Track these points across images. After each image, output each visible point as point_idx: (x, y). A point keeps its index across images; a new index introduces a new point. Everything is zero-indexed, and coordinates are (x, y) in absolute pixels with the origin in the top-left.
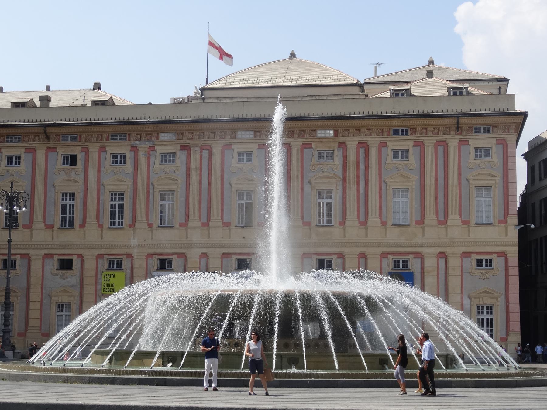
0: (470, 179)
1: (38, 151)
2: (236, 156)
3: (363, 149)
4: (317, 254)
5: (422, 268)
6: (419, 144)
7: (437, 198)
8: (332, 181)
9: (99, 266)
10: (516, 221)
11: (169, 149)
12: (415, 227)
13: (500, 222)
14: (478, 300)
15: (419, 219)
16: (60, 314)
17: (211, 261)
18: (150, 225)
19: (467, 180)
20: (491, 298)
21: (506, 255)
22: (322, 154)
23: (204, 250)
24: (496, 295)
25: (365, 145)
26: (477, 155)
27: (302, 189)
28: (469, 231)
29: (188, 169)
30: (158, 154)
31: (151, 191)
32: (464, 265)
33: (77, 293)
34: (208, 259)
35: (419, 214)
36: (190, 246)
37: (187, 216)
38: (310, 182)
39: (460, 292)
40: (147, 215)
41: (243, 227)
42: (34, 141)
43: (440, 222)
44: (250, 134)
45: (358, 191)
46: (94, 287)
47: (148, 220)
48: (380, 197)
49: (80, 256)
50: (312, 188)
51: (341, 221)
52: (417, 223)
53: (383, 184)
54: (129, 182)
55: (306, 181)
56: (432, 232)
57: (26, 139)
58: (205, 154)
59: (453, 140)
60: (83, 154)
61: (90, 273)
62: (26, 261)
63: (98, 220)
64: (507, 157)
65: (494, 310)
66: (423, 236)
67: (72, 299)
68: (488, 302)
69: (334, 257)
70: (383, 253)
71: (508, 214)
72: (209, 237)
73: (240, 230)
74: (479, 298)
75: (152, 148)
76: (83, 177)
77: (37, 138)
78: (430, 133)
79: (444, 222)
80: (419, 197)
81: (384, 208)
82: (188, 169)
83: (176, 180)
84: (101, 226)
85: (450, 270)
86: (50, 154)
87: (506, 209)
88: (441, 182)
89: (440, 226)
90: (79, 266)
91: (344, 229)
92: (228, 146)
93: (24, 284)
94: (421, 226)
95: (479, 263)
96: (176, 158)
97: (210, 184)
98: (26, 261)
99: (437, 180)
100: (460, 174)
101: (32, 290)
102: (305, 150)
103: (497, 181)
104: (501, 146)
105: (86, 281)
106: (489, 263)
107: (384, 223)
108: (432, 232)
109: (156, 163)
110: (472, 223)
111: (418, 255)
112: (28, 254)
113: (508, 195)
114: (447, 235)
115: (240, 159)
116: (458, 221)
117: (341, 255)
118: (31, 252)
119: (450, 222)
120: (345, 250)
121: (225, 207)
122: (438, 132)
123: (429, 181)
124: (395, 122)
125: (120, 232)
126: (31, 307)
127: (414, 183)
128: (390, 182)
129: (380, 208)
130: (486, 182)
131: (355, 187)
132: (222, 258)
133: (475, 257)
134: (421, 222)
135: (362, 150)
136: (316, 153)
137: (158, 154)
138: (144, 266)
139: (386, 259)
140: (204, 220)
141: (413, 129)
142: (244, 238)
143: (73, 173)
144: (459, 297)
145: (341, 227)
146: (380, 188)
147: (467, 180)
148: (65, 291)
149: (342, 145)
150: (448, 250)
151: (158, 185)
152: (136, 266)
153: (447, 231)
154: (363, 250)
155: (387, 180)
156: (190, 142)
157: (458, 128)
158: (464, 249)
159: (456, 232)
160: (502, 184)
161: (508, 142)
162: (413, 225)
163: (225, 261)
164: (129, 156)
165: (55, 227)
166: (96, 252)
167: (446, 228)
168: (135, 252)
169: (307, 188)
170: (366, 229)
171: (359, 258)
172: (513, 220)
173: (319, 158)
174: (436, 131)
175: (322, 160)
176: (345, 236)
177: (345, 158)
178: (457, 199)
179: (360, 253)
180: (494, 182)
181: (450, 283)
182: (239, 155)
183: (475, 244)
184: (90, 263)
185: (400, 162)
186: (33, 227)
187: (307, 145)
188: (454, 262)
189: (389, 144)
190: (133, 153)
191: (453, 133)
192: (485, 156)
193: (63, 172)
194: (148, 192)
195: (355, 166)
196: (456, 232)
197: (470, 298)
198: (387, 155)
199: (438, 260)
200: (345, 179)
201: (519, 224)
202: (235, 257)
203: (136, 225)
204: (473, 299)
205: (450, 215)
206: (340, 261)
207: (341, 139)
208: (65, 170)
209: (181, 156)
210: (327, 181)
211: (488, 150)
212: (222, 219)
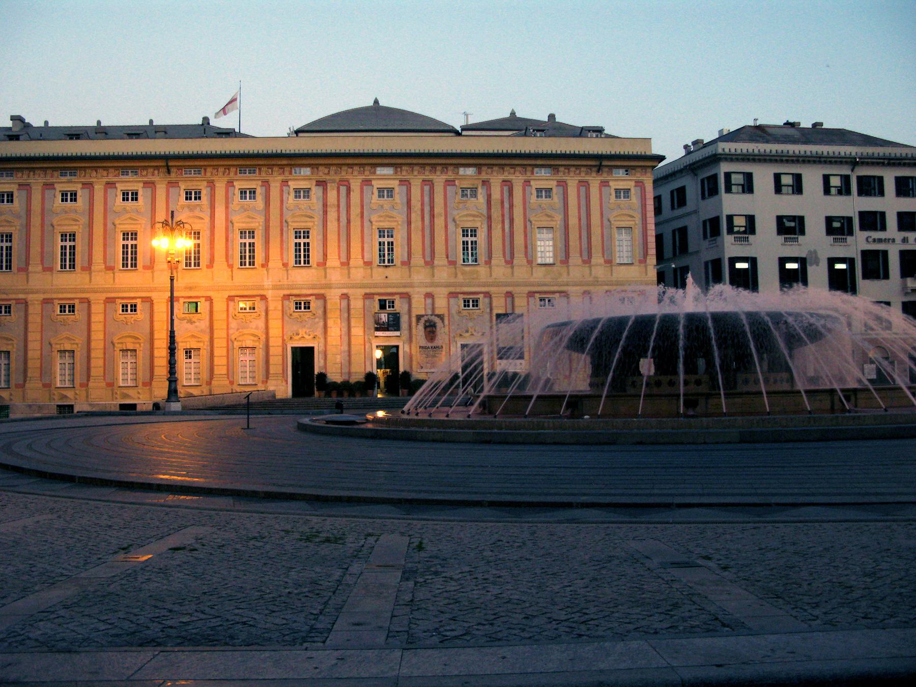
1: (158, 186)
2: (376, 192)
6: (563, 184)
7: (580, 237)
9: (231, 309)
10: (654, 261)
11: (303, 185)
13: (640, 262)
16: (189, 360)
17: (352, 303)
18: (285, 265)
23: (345, 291)
26: (616, 197)
27: (446, 227)
29: (325, 205)
30: (291, 189)
31: (285, 229)
33: (206, 338)
34: (349, 300)
35: (563, 255)
36: (329, 286)
37: (325, 255)
38: (454, 220)
40: (282, 254)
41: (386, 266)
42: (153, 175)
43: (584, 262)
44: (388, 171)
45: (503, 230)
46: (225, 331)
47: (282, 259)
48: (526, 236)
49: (209, 299)
50: (456, 226)
52: (562, 262)
53: (528, 223)
54: (261, 219)
56: (577, 271)
57: (145, 173)
58: (343, 189)
59: (595, 181)
60: (209, 189)
61: (220, 315)
62: (148, 304)
63: (227, 260)
66: (568, 274)
67: (202, 344)
69: (481, 296)
70: (529, 292)
72: (349, 277)
73: (381, 270)
75: (285, 183)
76: (209, 214)
77: (156, 172)
79: (587, 261)
81: (529, 247)
82: (325, 205)
83: (311, 217)
84: (231, 266)
86: (171, 189)
88: (584, 221)
90: (208, 308)
91: (490, 268)
92: (367, 182)
93: (148, 331)
96: (312, 193)
97: (349, 222)
98: (148, 305)
99: (580, 219)
101: (156, 336)
102: (448, 188)
104: (639, 188)
105: (216, 325)
107: (530, 262)
109: (291, 199)
112: (150, 298)
113: (646, 236)
115: (381, 195)
116: (602, 261)
117: (488, 295)
118: (154, 295)
119: (593, 261)
120: (492, 290)
121: (366, 246)
123: (573, 221)
125: (250, 271)
126: (156, 353)
129: (526, 247)
131: (500, 226)
134: (566, 261)
135: (506, 189)
137: (291, 189)
138: (280, 307)
140: (344, 260)
143: (198, 209)
146: (525, 227)
148: (193, 336)
149: (485, 183)
150: (591, 288)
152: (271, 308)
153: (591, 270)
154: (509, 289)
156: (328, 177)
157: (599, 169)
159: (600, 272)
160: (641, 226)
162: (558, 264)
163: (367, 302)
164: (259, 191)
165: (180, 268)
166: (226, 294)
167: (590, 267)
168: (269, 294)
169: (451, 226)
170: (512, 268)
172: (652, 260)
173: (463, 196)
175: (464, 199)
176: (491, 276)
177: (489, 197)
178: (600, 238)
179: (507, 293)
182: (379, 192)
184: (220, 306)
185: (544, 200)
186: (155, 268)
187: (450, 183)
189: (532, 183)
190: (264, 188)
191: (594, 174)
193: (186, 209)
194: (282, 230)
195: (499, 206)
200: (489, 218)
201: (658, 263)
202: (377, 298)
203: (270, 264)
206: (487, 300)
207: (484, 176)
208: (188, 207)
209: (316, 192)
210: (471, 219)
212: (363, 257)
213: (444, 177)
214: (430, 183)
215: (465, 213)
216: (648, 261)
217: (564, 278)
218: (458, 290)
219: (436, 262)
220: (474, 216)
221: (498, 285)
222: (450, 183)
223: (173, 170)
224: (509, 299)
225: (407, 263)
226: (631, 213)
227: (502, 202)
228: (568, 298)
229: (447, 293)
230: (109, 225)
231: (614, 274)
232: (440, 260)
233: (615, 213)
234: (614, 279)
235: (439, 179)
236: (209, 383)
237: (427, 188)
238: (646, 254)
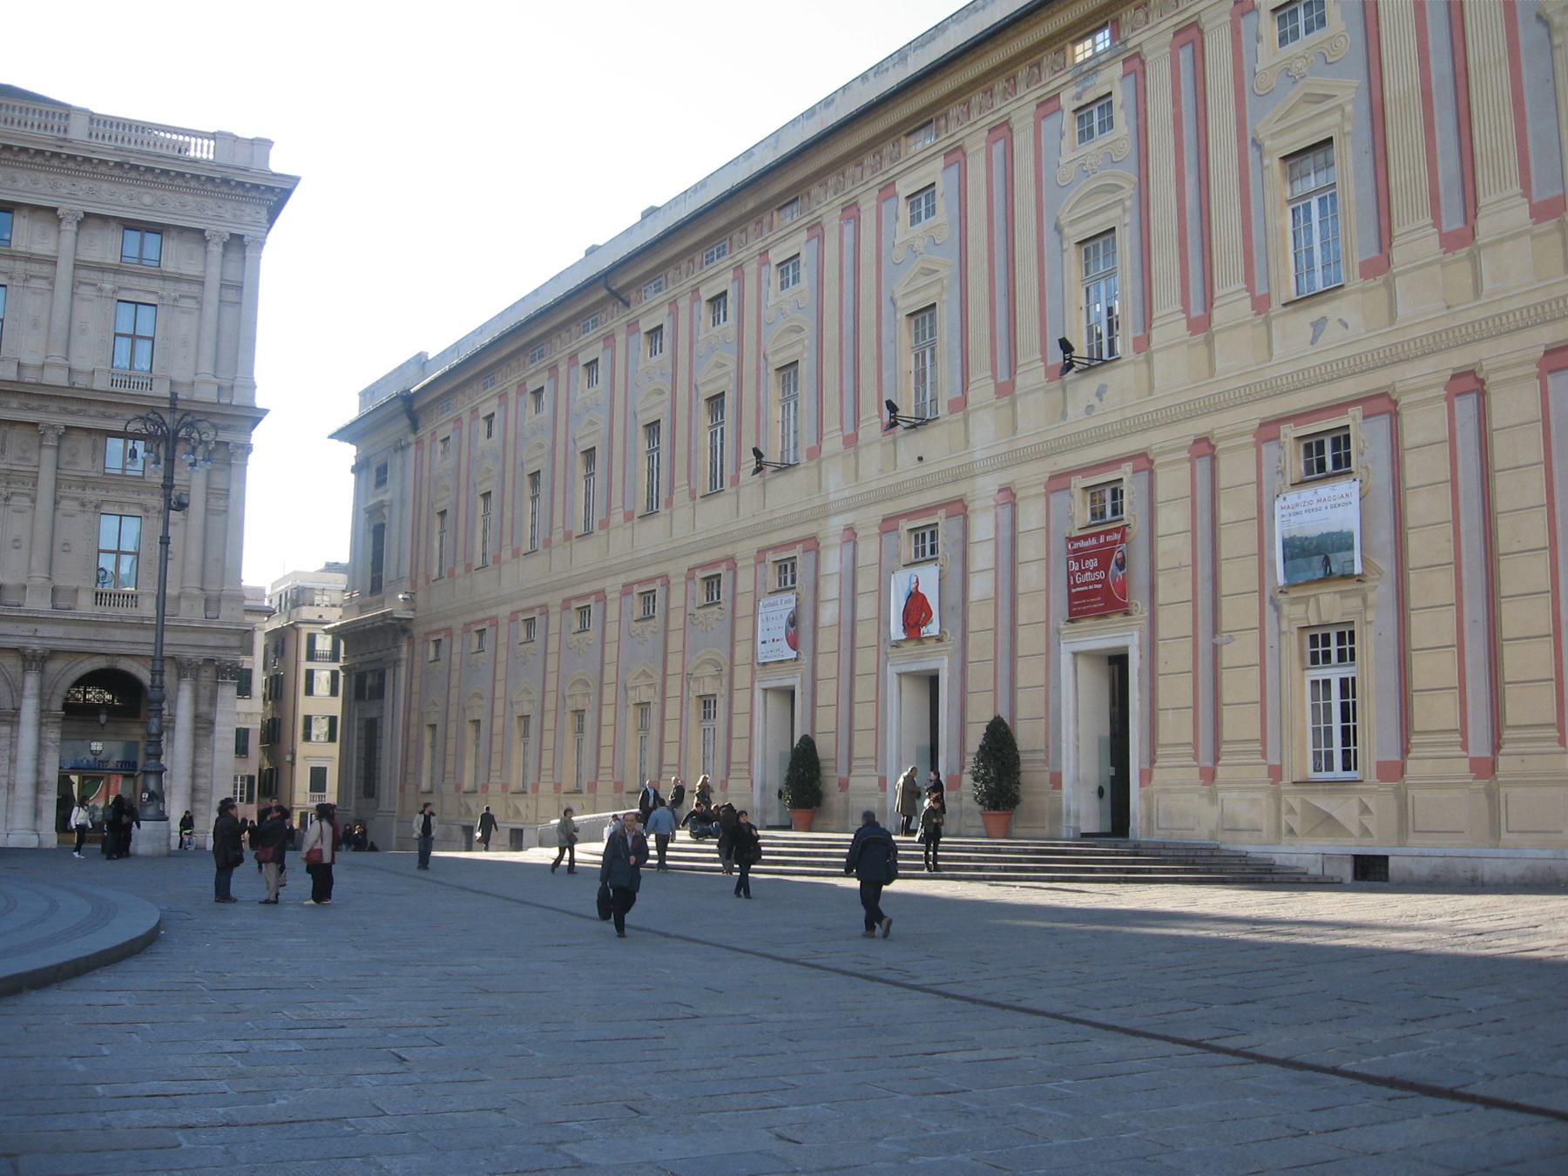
3: (1189, 49)
12: (1363, 291)
15: (1374, 253)
19: (1539, 17)
36: (824, 513)
43: (1451, 242)
51: (1140, 333)
53: (1252, 154)
55: (1048, 228)
56: (1425, 290)
58: (849, 229)
79: (1460, 240)
80: (1367, 161)
85: (1499, 444)
88: (1441, 66)
89: (1449, 257)
94: (1380, 279)
107: (1261, 305)
108: (1425, 290)
116: (1520, 214)
119: (1484, 225)
121: (885, 375)
123: (1400, 80)
128: (1273, 136)
132: (880, 536)
135: (1185, 55)
140: (849, 430)
142: (920, 459)
147: (1539, 17)
162: (1354, 281)
170: (1209, 343)
171: (1192, 460)
179: (1196, 442)
181: (1501, 504)
188: (1513, 405)
198: (1259, 39)
205: (1482, 201)
213: (1037, 93)
219: (1019, 380)
222: (1048, 105)
223: (633, 295)
224: (1203, 465)
228: (1394, 415)
230: (571, 444)
235: (1020, 107)
237: (998, 149)
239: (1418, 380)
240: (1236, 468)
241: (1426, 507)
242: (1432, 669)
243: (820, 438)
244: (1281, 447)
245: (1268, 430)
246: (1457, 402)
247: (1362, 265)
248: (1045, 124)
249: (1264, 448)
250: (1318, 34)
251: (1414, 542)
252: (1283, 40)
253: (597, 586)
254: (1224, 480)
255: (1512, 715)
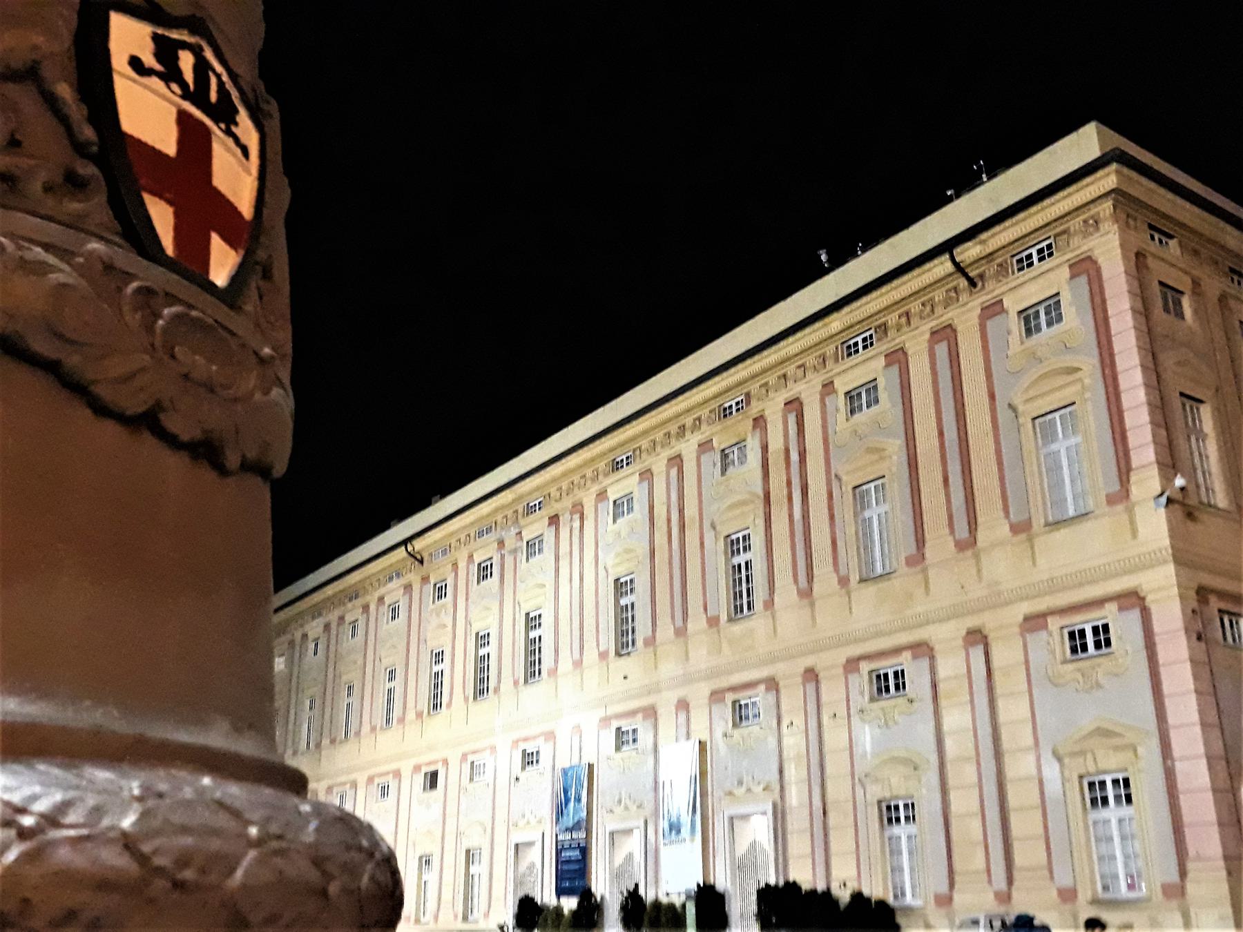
0: (1018, 402)
4: (733, 689)
5: (934, 686)
6: (898, 358)
8: (746, 509)
13: (1111, 500)
14: (1081, 760)
15: (913, 549)
19: (1010, 405)
20: (1116, 748)
21: (1143, 599)
22: (731, 456)
24: (1130, 737)
25: (796, 405)
27: (702, 544)
28: (1032, 548)
32: (1031, 658)
38: (713, 527)
39: (1030, 741)
43: (961, 546)
45: (791, 516)
53: (835, 484)
56: (948, 578)
59: (965, 315)
64: (1104, 301)
65: (1133, 790)
68: (1109, 765)
71: (1129, 469)
74: (1082, 753)
78: (915, 321)
79: (968, 544)
81: (840, 544)
84: (466, 699)
87: (1121, 454)
94: (919, 568)
95: (1077, 641)
99: (941, 434)
100: (992, 397)
103: (1087, 381)
104: (1083, 280)
106: (1103, 636)
107: (844, 581)
110: (1038, 523)
111: (922, 649)
114: (980, 578)
119: (981, 535)
122: (933, 311)
124: (835, 323)
127: (895, 457)
128: (848, 473)
129: (834, 543)
130: (1058, 395)
131: (785, 508)
133: (1054, 623)
134: (918, 558)
136: (718, 457)
139: (856, 675)
141: (879, 327)
144: (1031, 758)
145: (768, 613)
147: (1010, 405)
150: (987, 621)
151: (526, 601)
154: (809, 661)
155: (840, 473)
158: (1026, 608)
161: (1100, 261)
162: (903, 569)
167: (977, 557)
170: (812, 605)
172: (1147, 481)
174: (928, 308)
177: (765, 448)
180: (1078, 386)
181: (1002, 718)
183: (1053, 586)
188: (1006, 654)
189: (837, 383)
192: (1049, 324)
196: (1002, 563)
197: (1059, 759)
198: (837, 410)
199: (968, 654)
204: (1066, 761)
205: (980, 520)
206: (771, 698)
210: (738, 512)
211: (1053, 307)
214: (677, 461)
215: (729, 502)
216: (1135, 490)
217: (920, 607)
218: (725, 682)
219: (689, 626)
220: (743, 503)
221: (788, 655)
224: (811, 687)
225: (651, 642)
226: (1069, 361)
227: (787, 451)
228: (932, 658)
229: (707, 693)
231: (1041, 561)
232: (697, 623)
233: (1026, 380)
234: (1045, 577)
236: (436, 918)
238: (1124, 469)
239: (947, 636)
240: (832, 692)
241: (956, 719)
242: (968, 828)
243: (556, 661)
244: (861, 676)
245: (852, 665)
246: (971, 651)
247: (906, 558)
248: (703, 458)
249: (850, 676)
250: (874, 408)
251: (949, 743)
252: (852, 412)
253: (394, 766)
254: (825, 698)
255: (1018, 860)
